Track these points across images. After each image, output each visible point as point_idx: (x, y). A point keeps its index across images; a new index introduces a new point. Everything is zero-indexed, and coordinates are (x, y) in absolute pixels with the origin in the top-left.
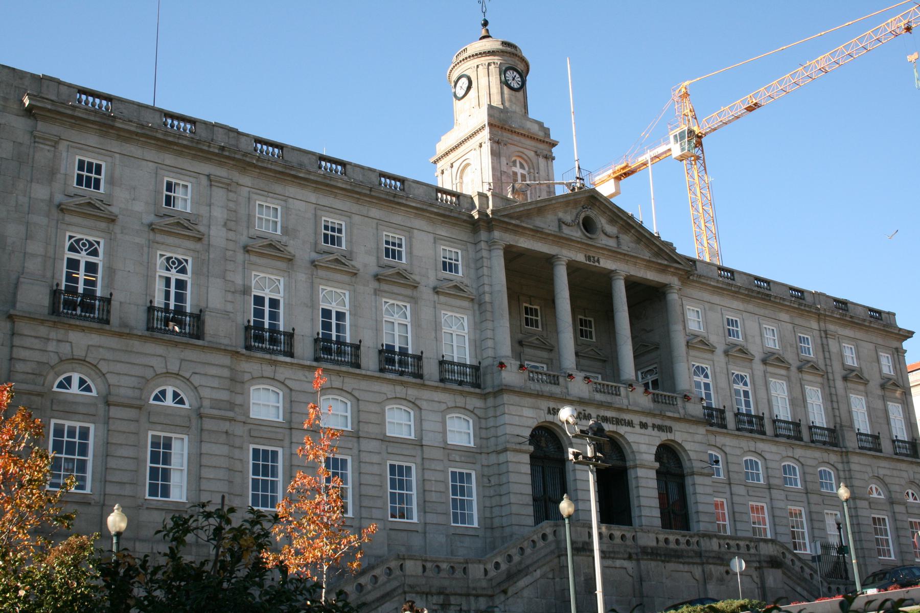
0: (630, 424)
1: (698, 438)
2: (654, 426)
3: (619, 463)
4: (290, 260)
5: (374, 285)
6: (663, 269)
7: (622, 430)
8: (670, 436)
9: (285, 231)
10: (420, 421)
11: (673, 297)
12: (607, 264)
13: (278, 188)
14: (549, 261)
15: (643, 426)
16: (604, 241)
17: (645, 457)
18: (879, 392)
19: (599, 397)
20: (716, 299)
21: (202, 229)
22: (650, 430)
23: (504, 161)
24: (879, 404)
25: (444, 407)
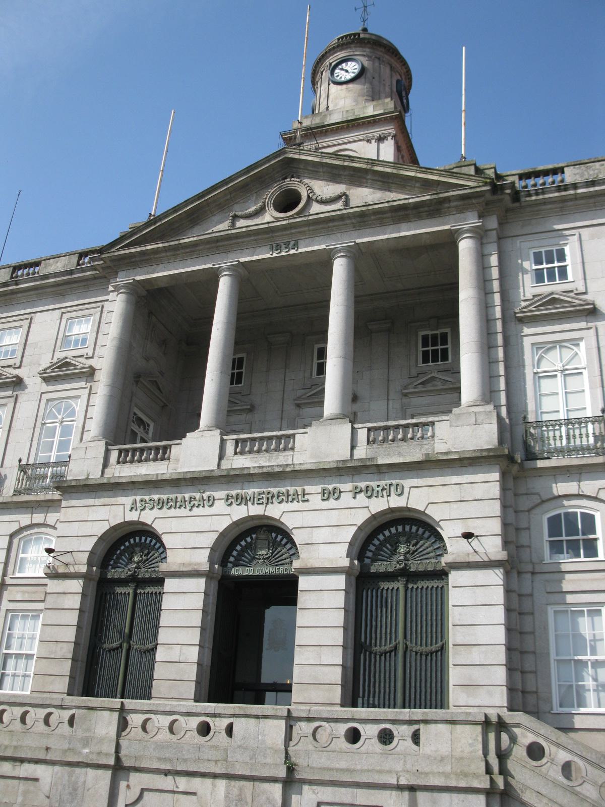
1: (479, 491)
2: (356, 492)
3: (282, 570)
6: (433, 210)
7: (275, 511)
8: (396, 502)
22: (346, 499)
25: (15, 527)
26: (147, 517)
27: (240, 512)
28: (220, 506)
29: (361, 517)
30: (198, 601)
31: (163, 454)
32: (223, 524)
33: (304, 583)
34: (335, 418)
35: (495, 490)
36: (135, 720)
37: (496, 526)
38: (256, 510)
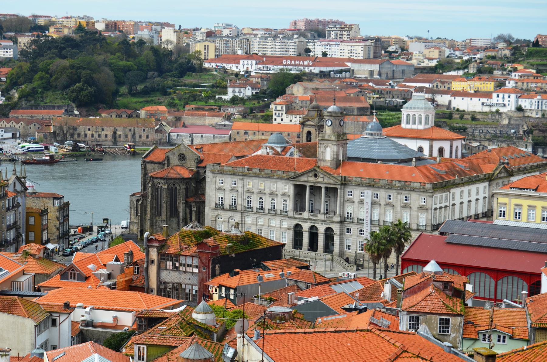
0: (318, 223)
4: (253, 192)
5: (269, 195)
7: (316, 225)
8: (329, 226)
9: (253, 187)
10: (276, 222)
11: (339, 191)
12: (319, 185)
13: (251, 178)
14: (305, 187)
15: (322, 224)
16: (320, 180)
17: (321, 231)
18: (417, 209)
19: (311, 218)
20: (357, 187)
21: (237, 189)
22: (323, 225)
23: (322, 149)
24: (416, 213)
26: (300, 223)
27: (312, 224)
28: (309, 223)
29: (325, 227)
30: (307, 235)
31: (301, 214)
32: (310, 226)
33: (319, 234)
34: (323, 213)
35: (339, 227)
36: (301, 252)
37: (339, 231)
38: (313, 224)
